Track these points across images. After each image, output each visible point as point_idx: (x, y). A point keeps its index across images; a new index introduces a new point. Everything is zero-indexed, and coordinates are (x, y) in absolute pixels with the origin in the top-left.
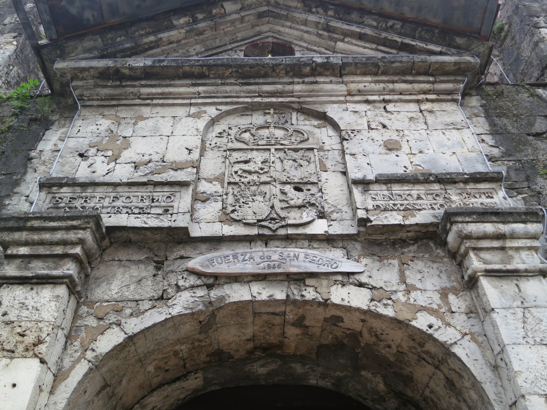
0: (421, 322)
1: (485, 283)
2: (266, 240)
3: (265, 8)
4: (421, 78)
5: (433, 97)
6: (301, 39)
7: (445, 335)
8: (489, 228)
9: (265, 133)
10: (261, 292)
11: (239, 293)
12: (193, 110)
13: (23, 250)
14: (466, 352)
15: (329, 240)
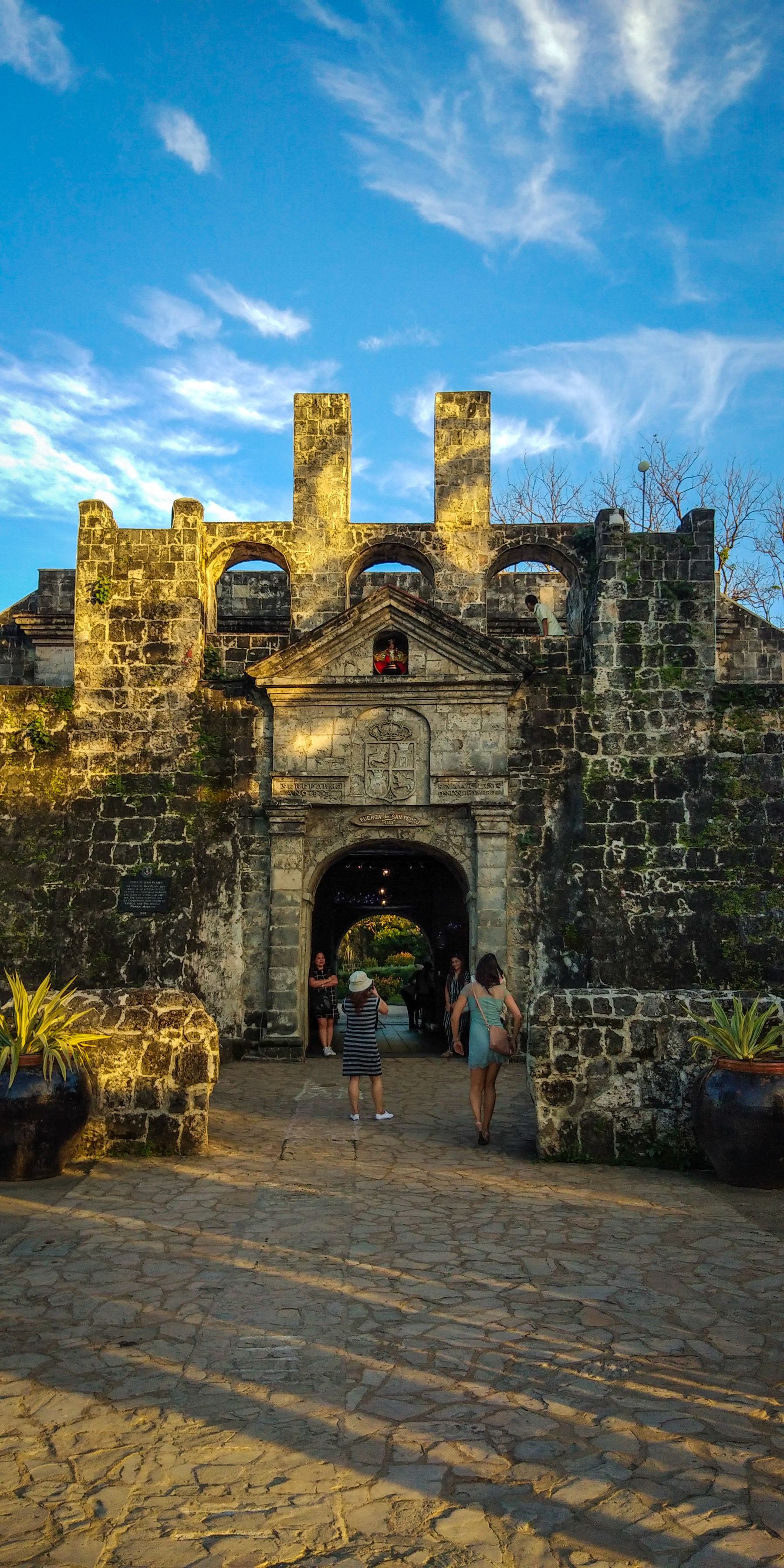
0: (451, 852)
1: (479, 838)
2: (385, 806)
3: (386, 603)
4: (485, 688)
5: (490, 700)
6: (414, 631)
7: (460, 857)
8: (487, 812)
9: (386, 728)
10: (383, 835)
11: (375, 835)
12: (344, 710)
13: (279, 820)
14: (466, 866)
15: (417, 807)
